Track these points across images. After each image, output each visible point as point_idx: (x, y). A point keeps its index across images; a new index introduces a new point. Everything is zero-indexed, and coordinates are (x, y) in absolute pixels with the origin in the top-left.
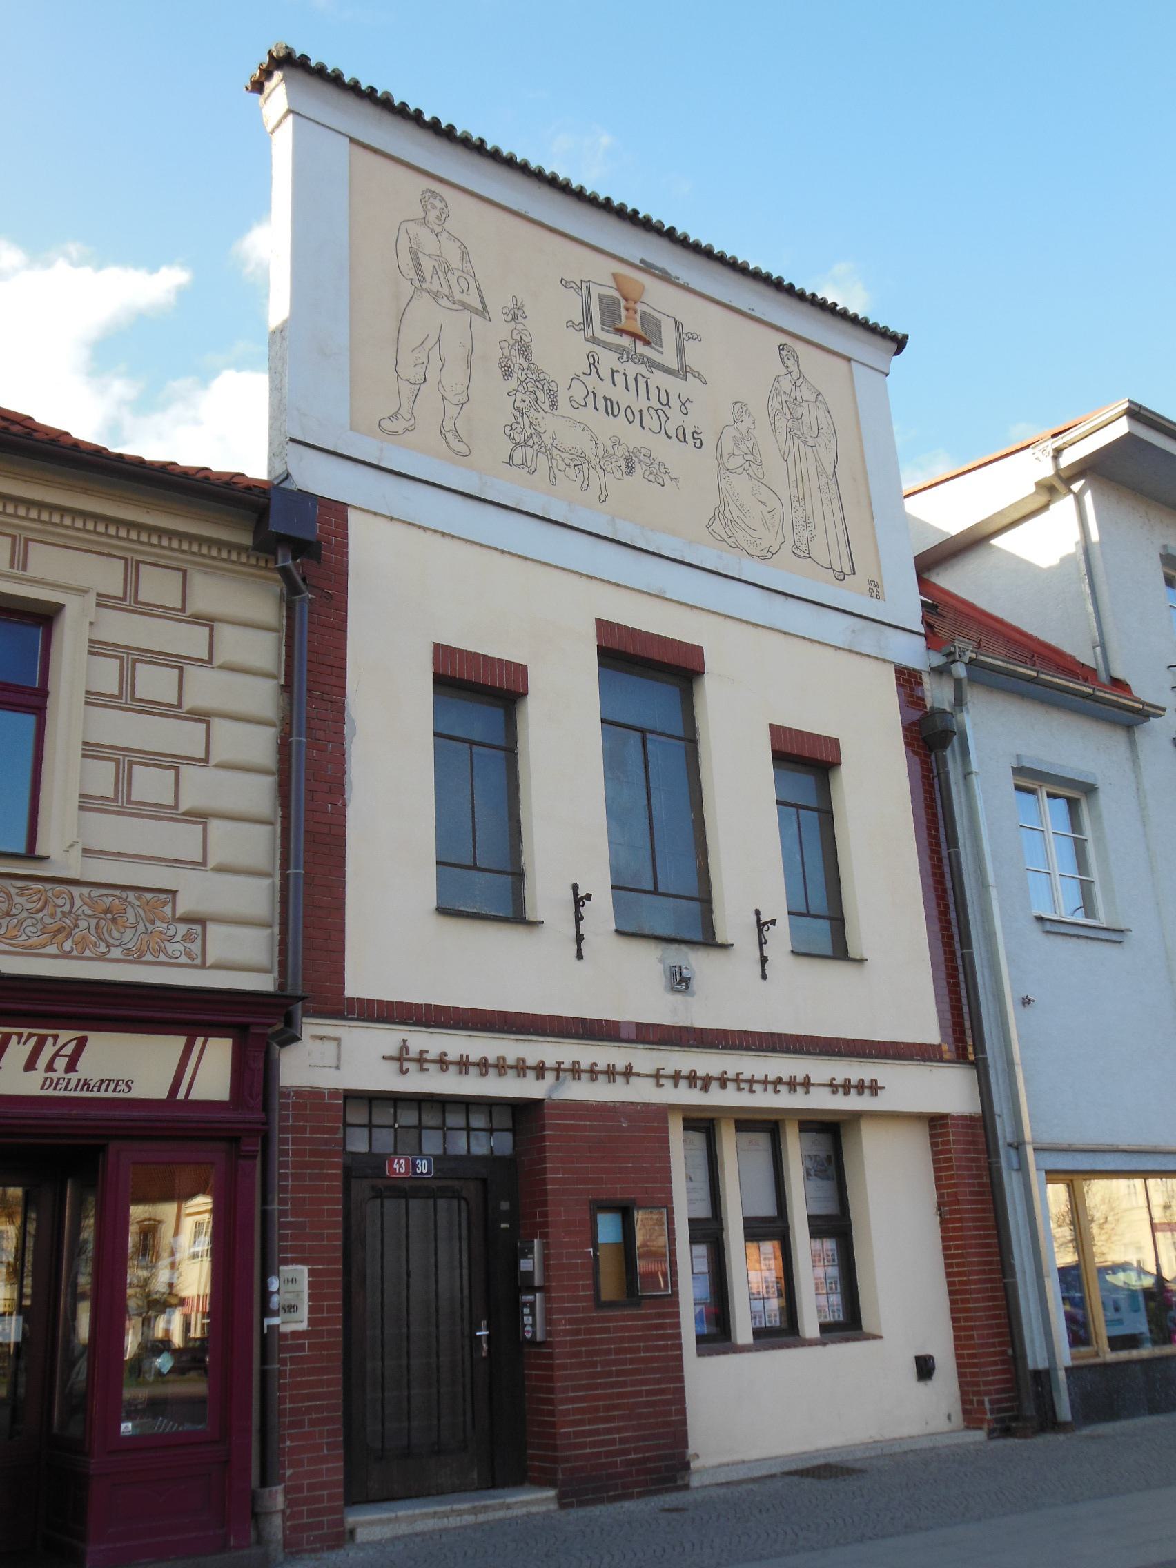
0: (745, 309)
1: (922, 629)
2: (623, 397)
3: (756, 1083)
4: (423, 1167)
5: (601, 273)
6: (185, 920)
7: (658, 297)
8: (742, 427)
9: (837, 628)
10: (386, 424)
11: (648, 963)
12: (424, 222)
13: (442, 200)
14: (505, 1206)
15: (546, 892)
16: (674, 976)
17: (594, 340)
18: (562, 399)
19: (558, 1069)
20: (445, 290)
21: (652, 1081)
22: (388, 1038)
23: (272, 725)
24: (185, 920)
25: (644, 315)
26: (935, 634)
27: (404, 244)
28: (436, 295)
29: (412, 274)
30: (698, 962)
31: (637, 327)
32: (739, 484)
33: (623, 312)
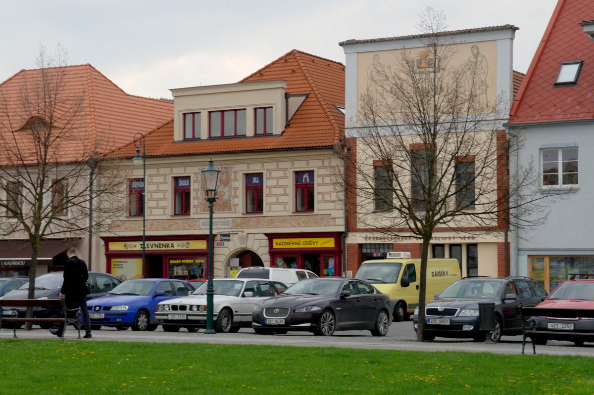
6: (333, 218)
13: (378, 55)
22: (364, 235)
24: (333, 218)
27: (369, 71)
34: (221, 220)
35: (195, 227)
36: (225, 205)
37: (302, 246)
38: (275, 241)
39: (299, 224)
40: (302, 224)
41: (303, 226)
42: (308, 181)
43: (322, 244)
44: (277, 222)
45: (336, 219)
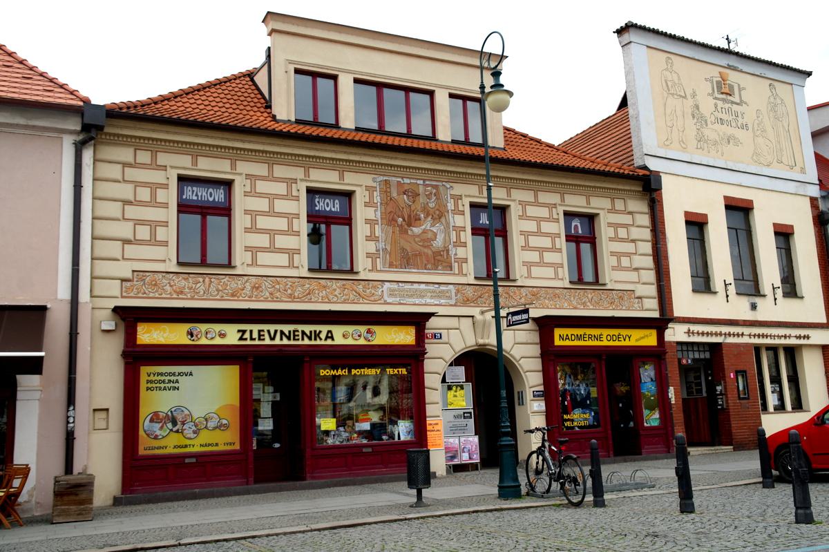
0: (759, 74)
1: (818, 182)
2: (725, 117)
3: (778, 337)
4: (690, 362)
5: (714, 72)
6: (638, 298)
7: (733, 77)
8: (760, 119)
9: (791, 187)
10: (666, 143)
11: (745, 302)
12: (667, 69)
14: (710, 372)
15: (717, 284)
16: (752, 306)
17: (716, 98)
18: (709, 123)
19: (725, 334)
20: (675, 92)
21: (748, 337)
22: (685, 327)
23: (649, 241)
25: (729, 84)
26: (822, 183)
27: (663, 79)
28: (673, 94)
29: (666, 89)
30: (758, 300)
31: (727, 90)
32: (760, 140)
33: (723, 86)
34: (431, 287)
35: (372, 298)
36: (439, 258)
37: (605, 343)
38: (558, 332)
39: (584, 304)
40: (589, 304)
41: (591, 307)
42: (580, 232)
43: (637, 340)
44: (545, 298)
45: (644, 300)
